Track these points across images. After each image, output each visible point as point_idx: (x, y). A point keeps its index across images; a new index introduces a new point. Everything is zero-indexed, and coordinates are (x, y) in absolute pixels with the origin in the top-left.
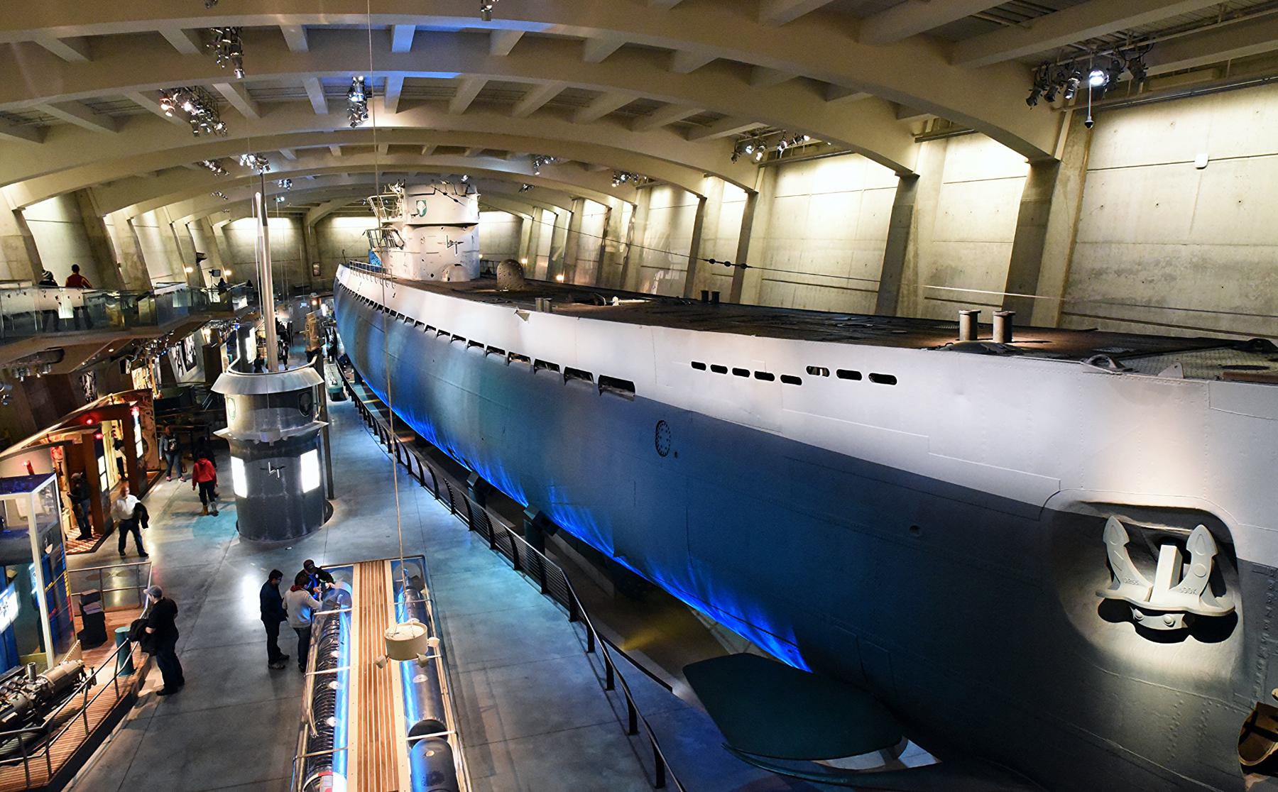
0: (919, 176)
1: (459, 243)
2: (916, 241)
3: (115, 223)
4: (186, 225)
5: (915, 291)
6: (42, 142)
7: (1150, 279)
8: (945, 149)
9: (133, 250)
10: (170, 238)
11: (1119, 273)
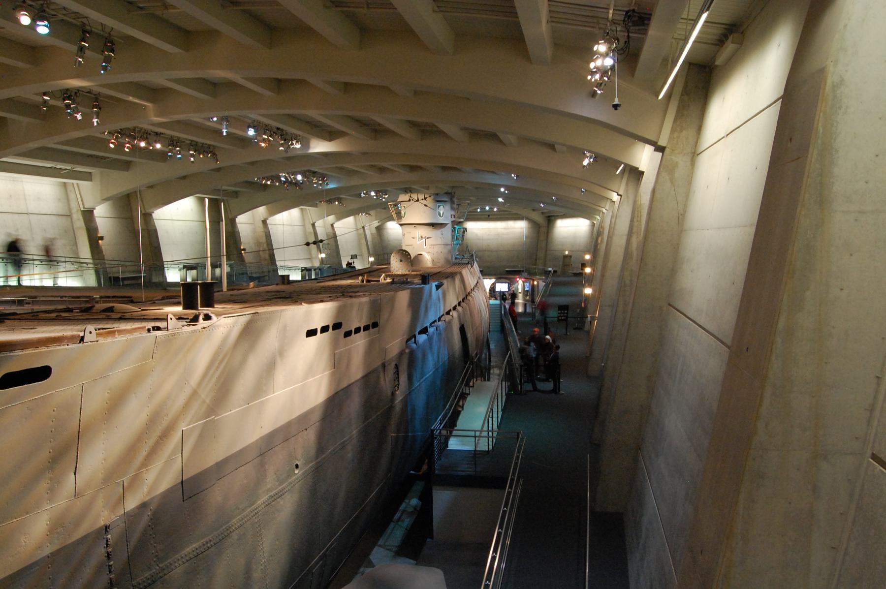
0: (643, 172)
1: (428, 238)
3: (246, 223)
4: (332, 225)
6: (127, 171)
9: (263, 240)
10: (311, 233)
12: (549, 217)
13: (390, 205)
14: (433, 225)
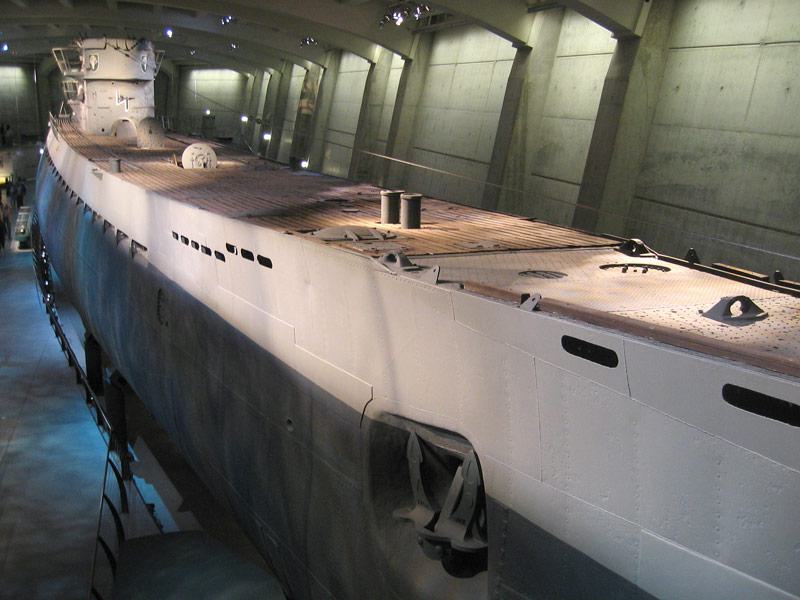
0: (531, 48)
2: (525, 116)
5: (522, 166)
7: (708, 166)
8: (560, 22)
11: (684, 158)
12: (180, 66)
13: (57, 52)
14: (135, 82)
